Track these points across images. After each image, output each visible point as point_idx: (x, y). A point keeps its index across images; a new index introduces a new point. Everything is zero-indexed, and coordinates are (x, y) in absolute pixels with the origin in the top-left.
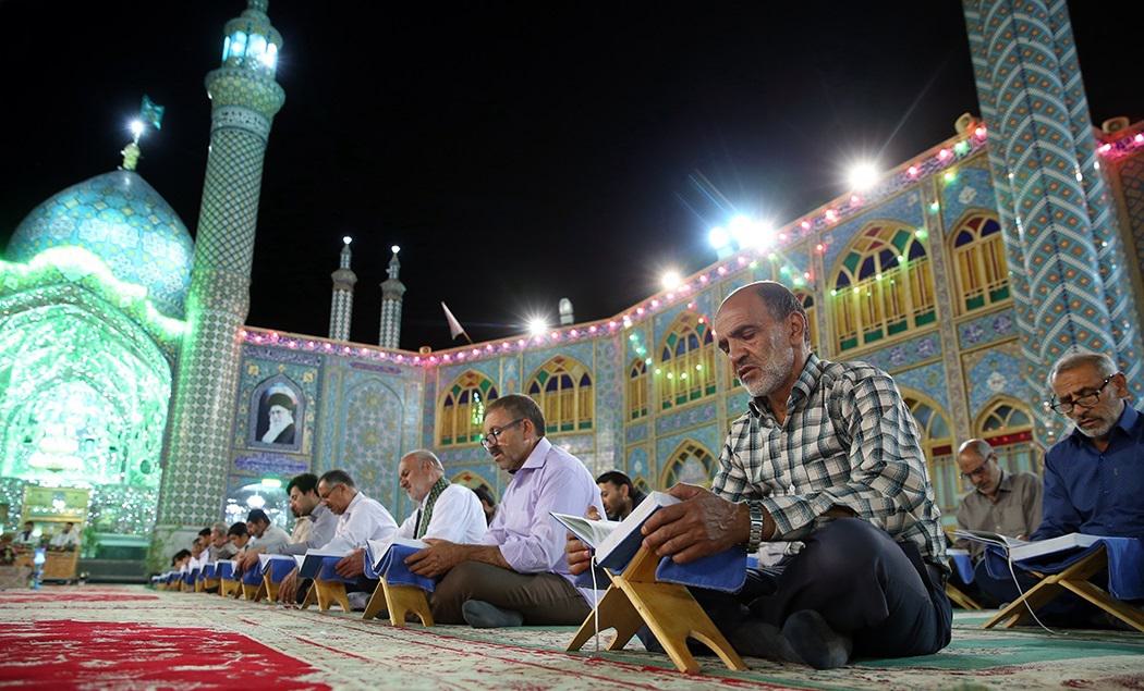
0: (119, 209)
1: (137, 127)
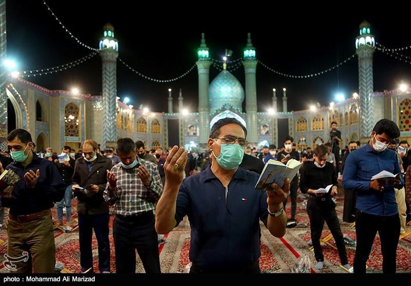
0: (226, 83)
1: (225, 59)
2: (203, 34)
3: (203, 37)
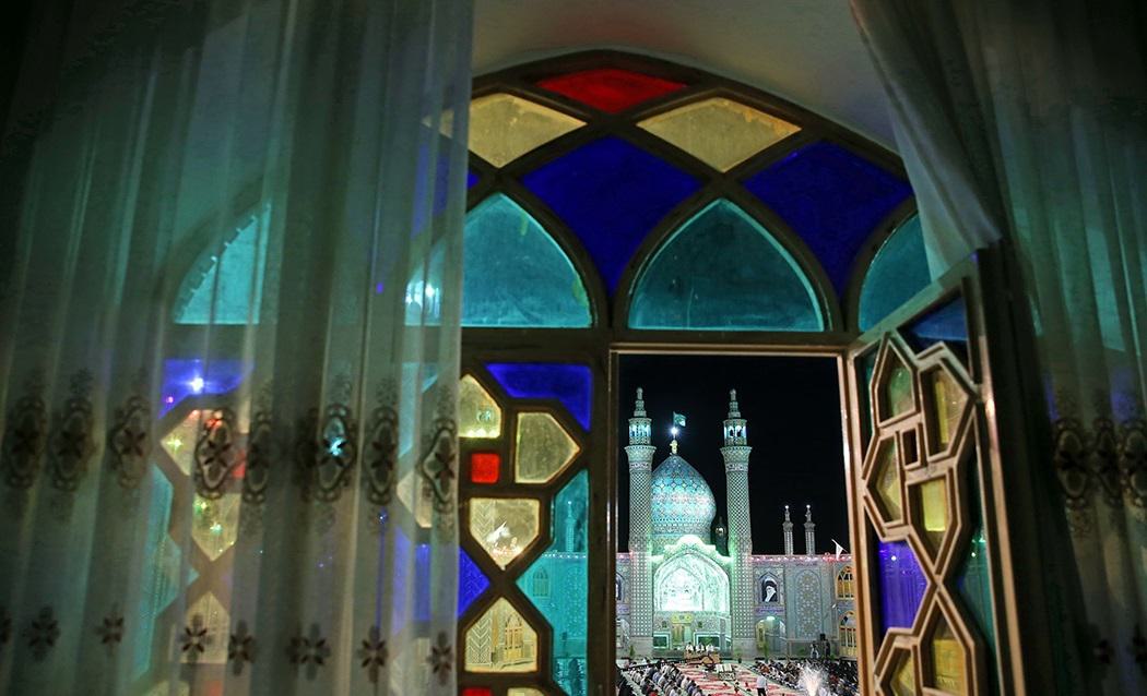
1: (674, 431)
2: (640, 391)
3: (640, 396)
